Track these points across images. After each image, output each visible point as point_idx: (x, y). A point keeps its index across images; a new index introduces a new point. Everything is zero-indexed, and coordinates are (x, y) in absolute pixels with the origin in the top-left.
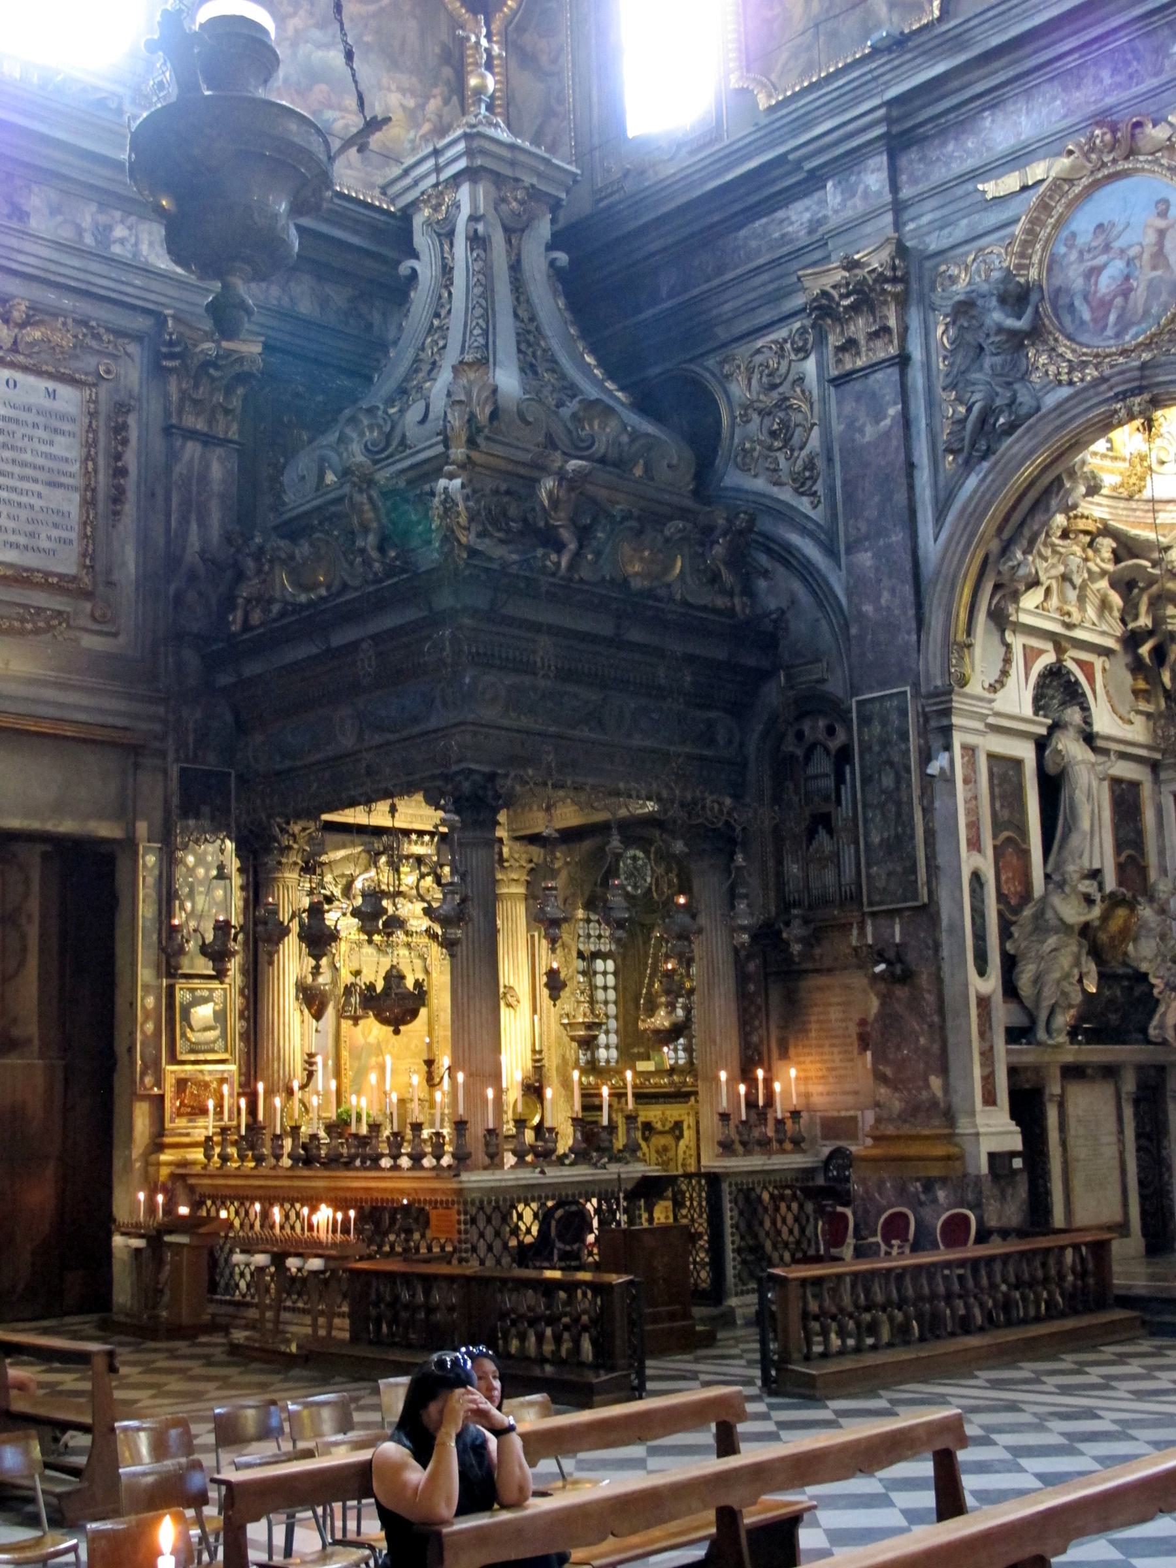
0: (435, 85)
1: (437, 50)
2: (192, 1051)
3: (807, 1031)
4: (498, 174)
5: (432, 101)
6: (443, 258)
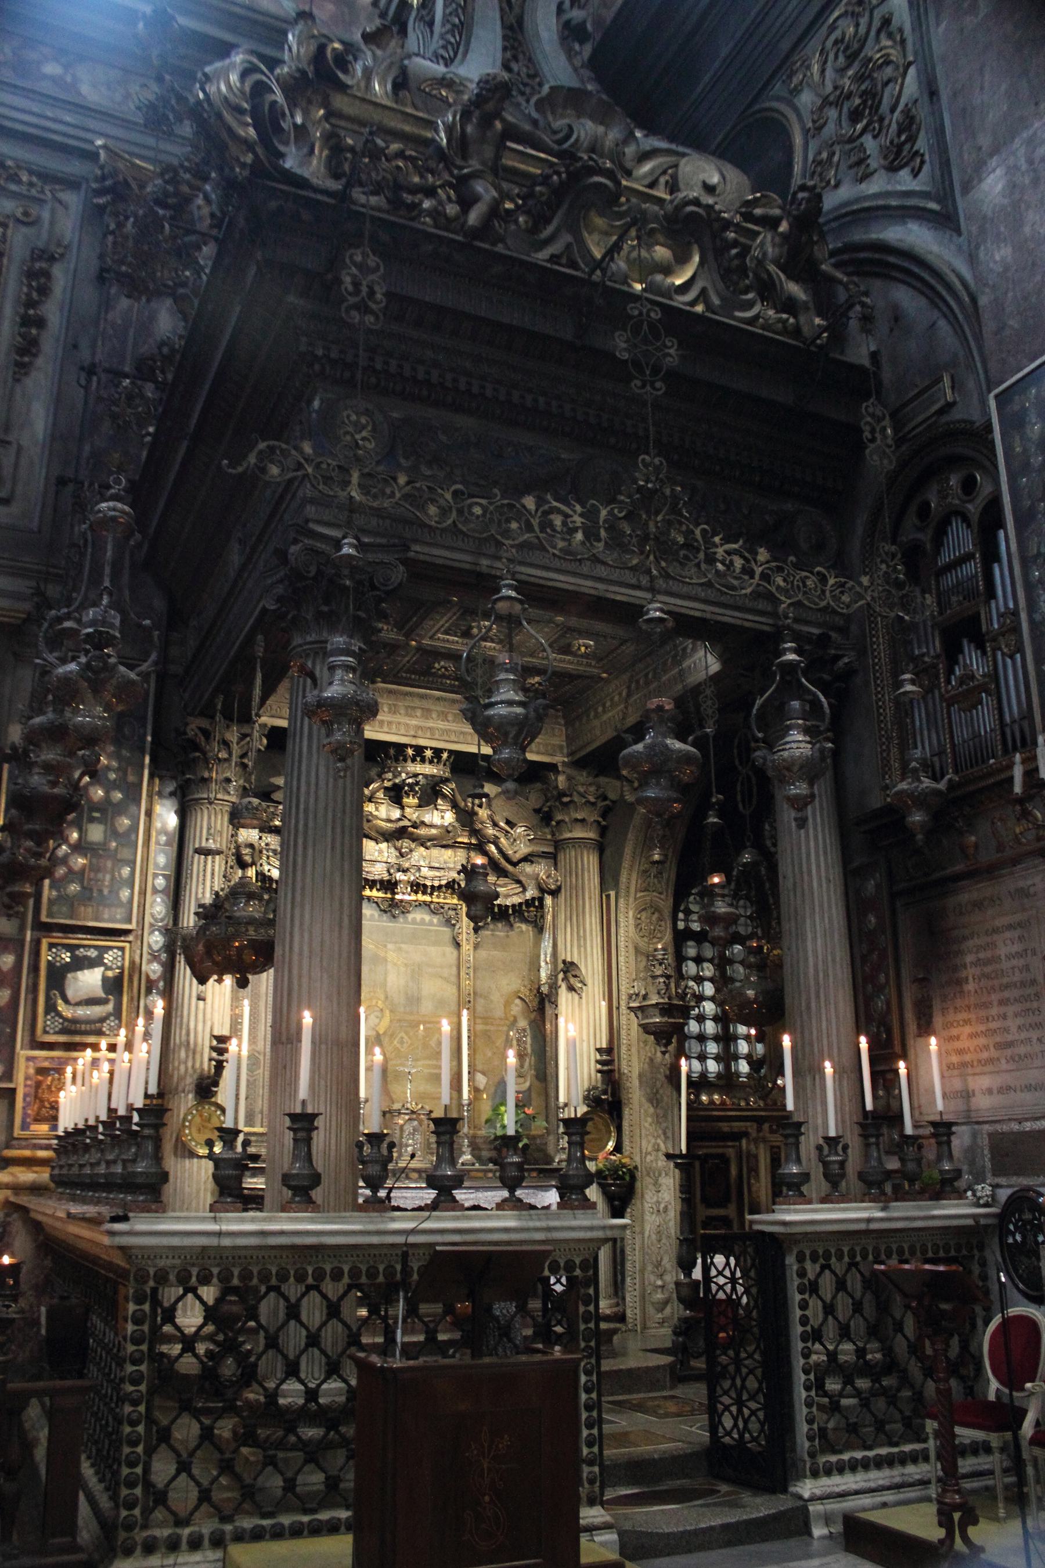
2: (63, 1031)
3: (960, 982)
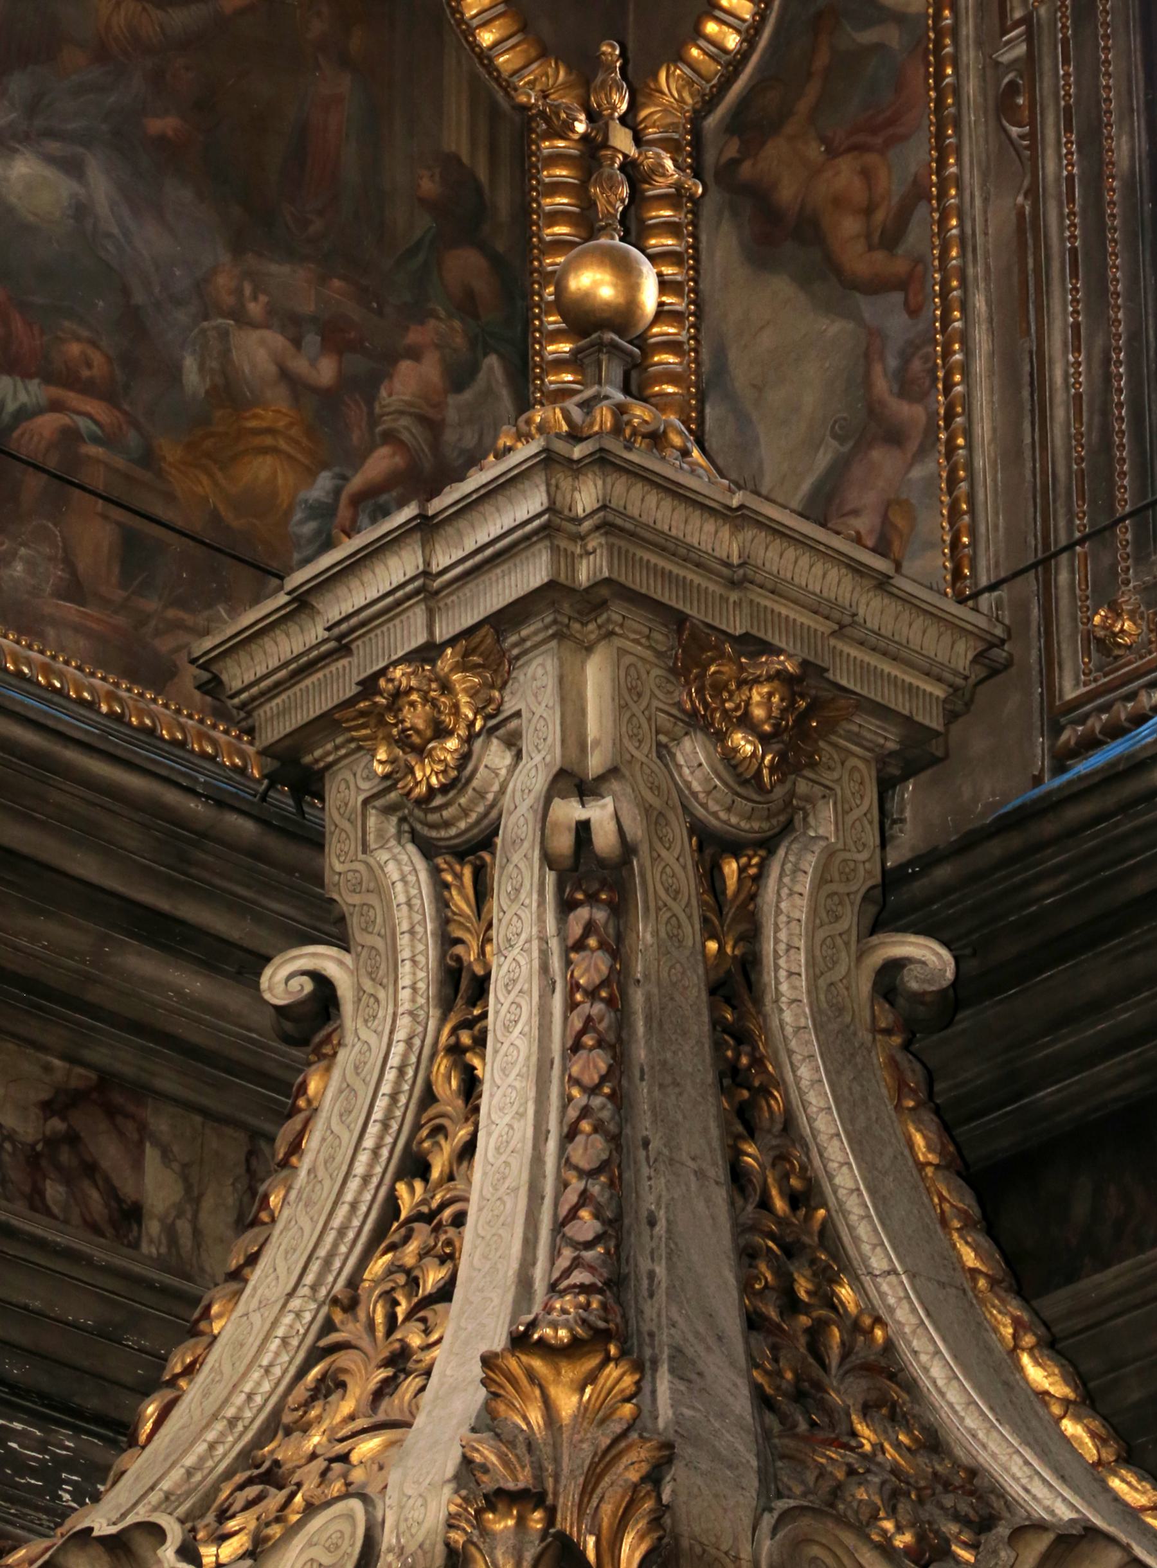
0: (418, 312)
1: (429, 186)
5: (405, 366)
6: (447, 941)
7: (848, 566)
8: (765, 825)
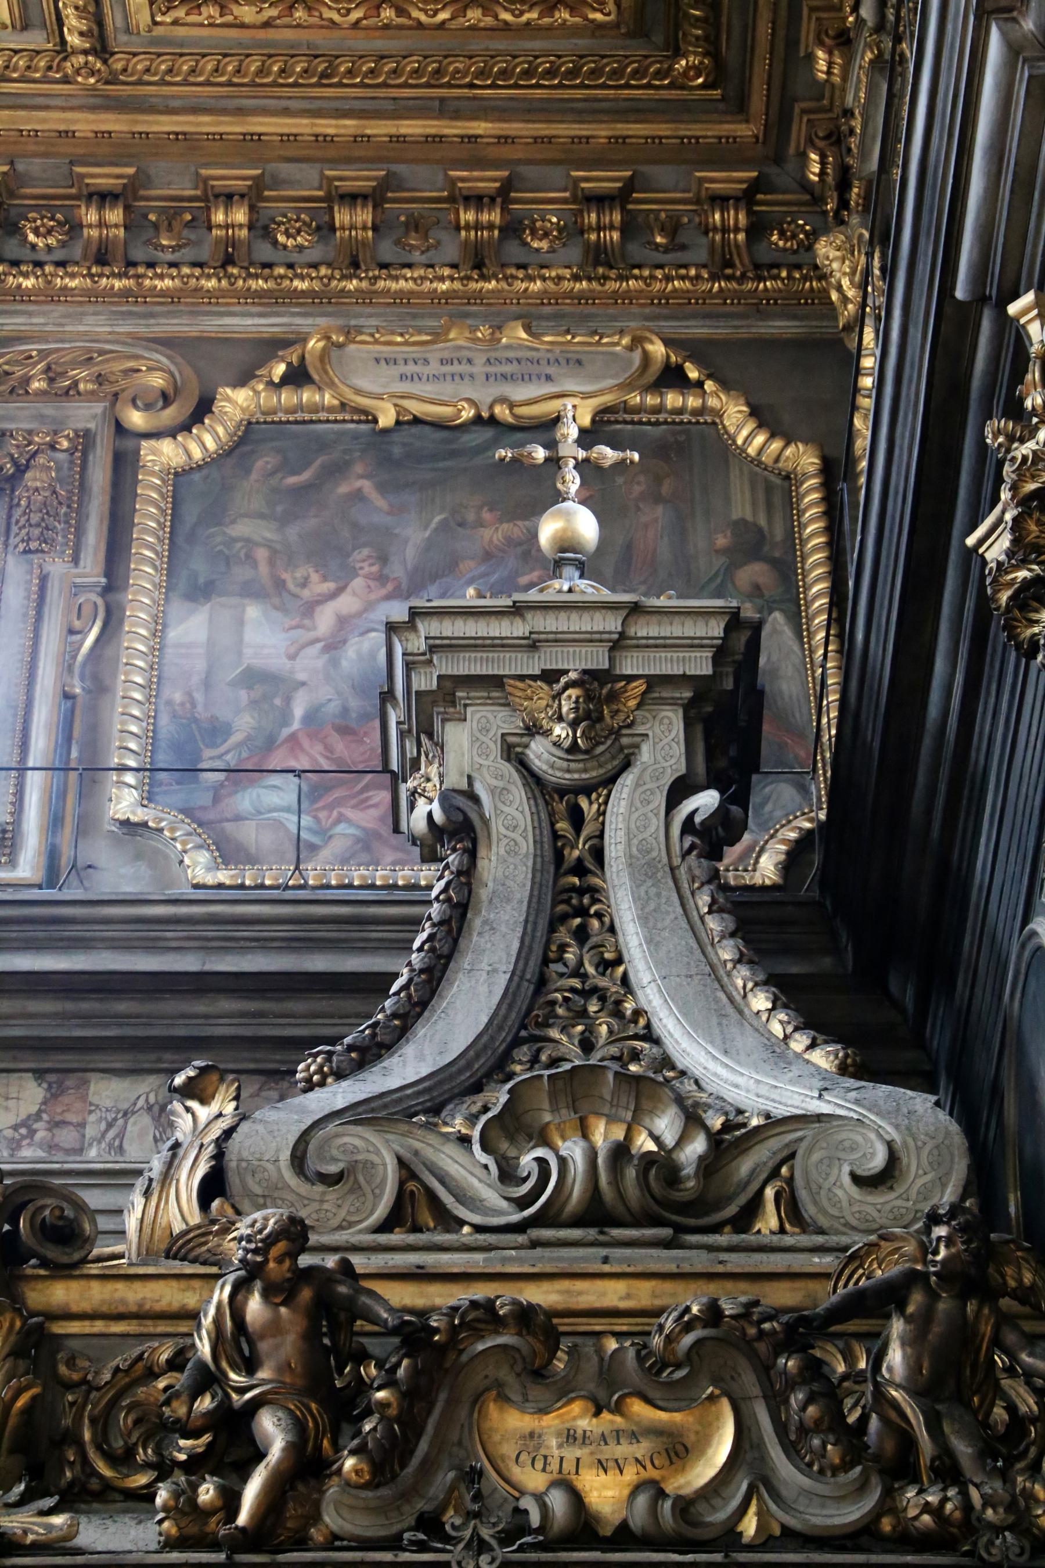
4: (496, 682)
7: (604, 608)
8: (601, 771)
